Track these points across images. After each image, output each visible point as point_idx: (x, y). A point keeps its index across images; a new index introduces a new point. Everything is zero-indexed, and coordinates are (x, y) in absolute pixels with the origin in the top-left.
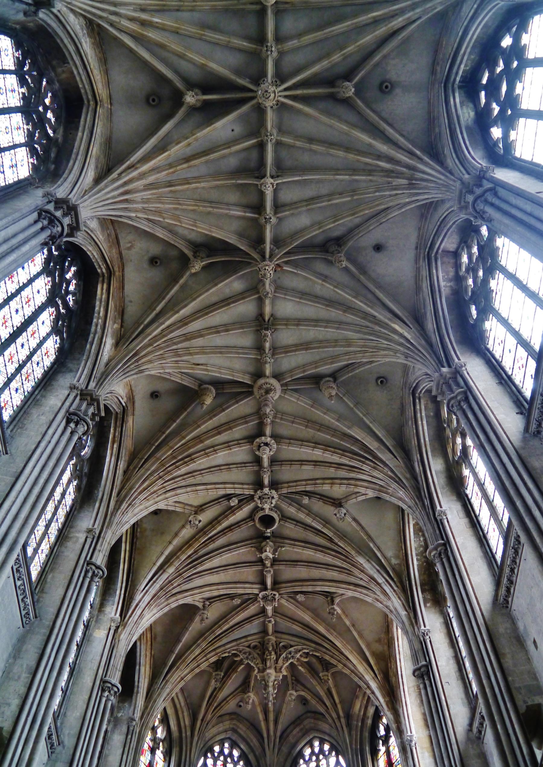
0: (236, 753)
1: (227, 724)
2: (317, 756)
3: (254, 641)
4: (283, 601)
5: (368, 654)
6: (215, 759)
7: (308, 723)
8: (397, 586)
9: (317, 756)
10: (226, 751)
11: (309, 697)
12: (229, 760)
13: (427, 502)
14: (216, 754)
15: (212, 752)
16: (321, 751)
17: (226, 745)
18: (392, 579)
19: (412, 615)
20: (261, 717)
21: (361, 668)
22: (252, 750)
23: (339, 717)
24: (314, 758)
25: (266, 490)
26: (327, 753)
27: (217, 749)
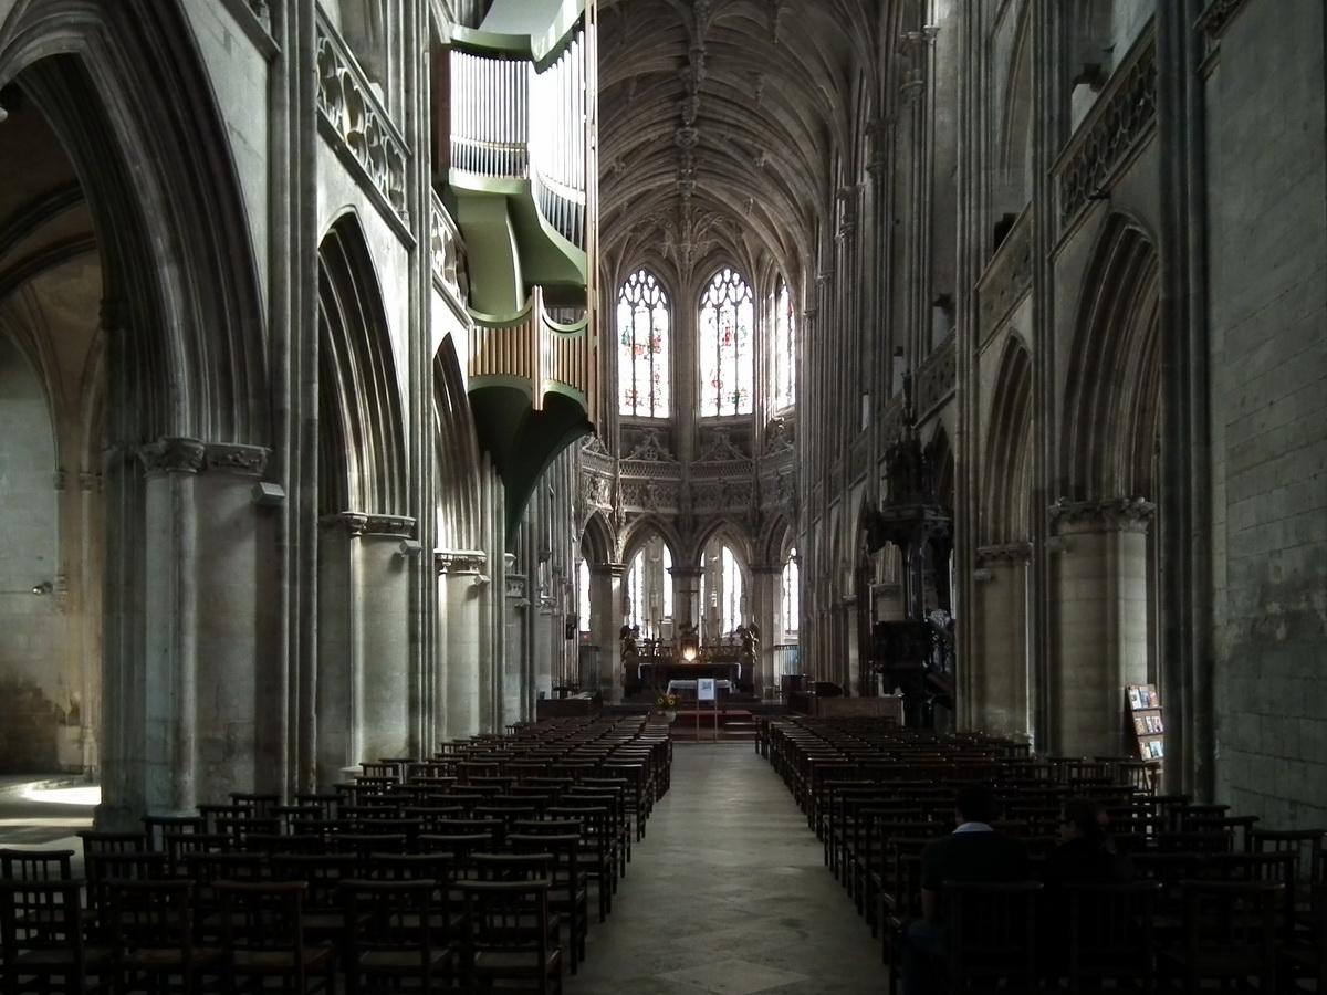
0: (651, 280)
1: (643, 260)
2: (727, 284)
3: (669, 205)
4: (700, 185)
5: (780, 234)
6: (633, 288)
7: (720, 258)
8: (806, 225)
9: (727, 284)
10: (642, 279)
11: (722, 244)
12: (645, 287)
13: (832, 217)
14: (633, 284)
15: (630, 282)
16: (731, 281)
17: (642, 273)
18: (802, 217)
19: (814, 259)
20: (675, 256)
21: (771, 244)
22: (667, 280)
23: (749, 263)
24: (724, 285)
25: (687, 129)
26: (736, 283)
27: (633, 278)
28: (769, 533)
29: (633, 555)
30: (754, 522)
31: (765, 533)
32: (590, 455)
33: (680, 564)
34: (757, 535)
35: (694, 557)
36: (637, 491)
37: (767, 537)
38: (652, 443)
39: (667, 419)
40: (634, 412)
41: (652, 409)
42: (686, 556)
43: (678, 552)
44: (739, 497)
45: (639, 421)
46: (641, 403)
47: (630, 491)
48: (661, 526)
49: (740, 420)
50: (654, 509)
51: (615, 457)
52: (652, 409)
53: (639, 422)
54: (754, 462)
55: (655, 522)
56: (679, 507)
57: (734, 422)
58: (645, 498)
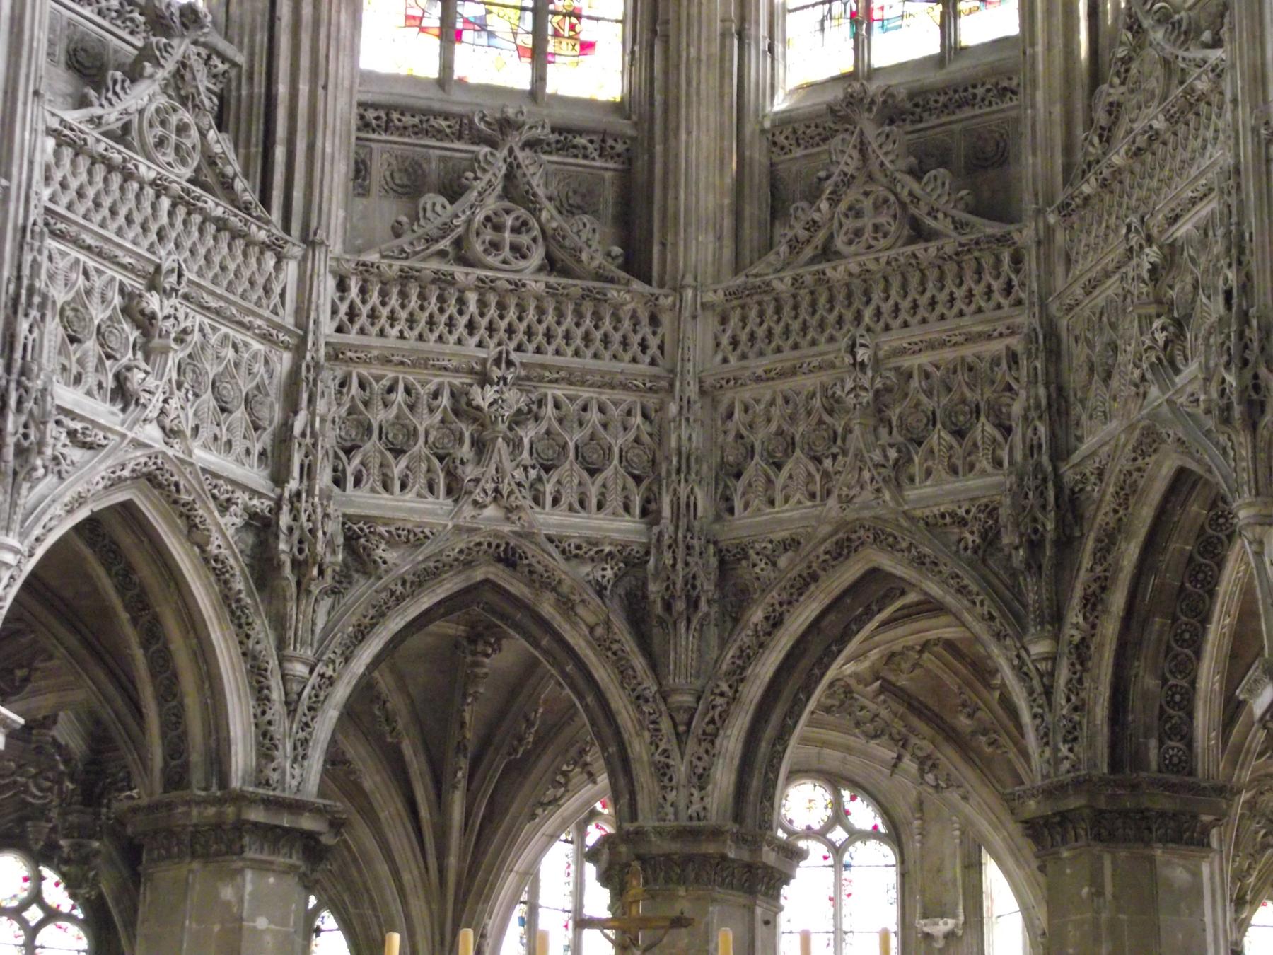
28: (1118, 600)
29: (511, 837)
30: (1034, 546)
31: (1093, 603)
32: (128, 176)
33: (647, 820)
34: (1057, 618)
35: (724, 777)
36: (425, 422)
37: (1110, 628)
38: (513, 189)
39: (616, 108)
40: (447, 64)
41: (538, 55)
42: (681, 770)
43: (639, 748)
44: (959, 434)
45: (457, 95)
46: (481, 26)
47: (379, 416)
48: (547, 608)
49: (957, 69)
50: (509, 510)
51: (309, 241)
52: (538, 55)
53: (457, 102)
54: (1026, 235)
55: (517, 588)
56: (649, 512)
57: (935, 77)
58: (466, 451)
